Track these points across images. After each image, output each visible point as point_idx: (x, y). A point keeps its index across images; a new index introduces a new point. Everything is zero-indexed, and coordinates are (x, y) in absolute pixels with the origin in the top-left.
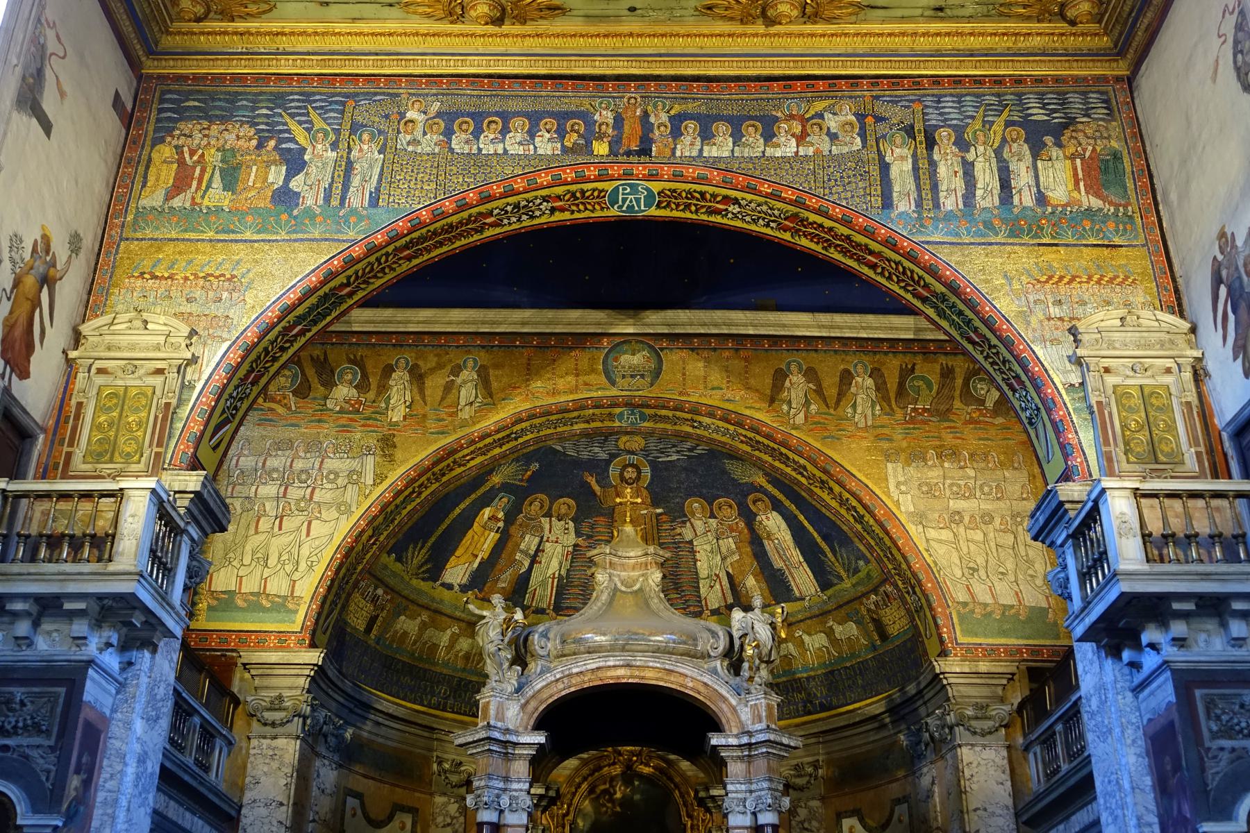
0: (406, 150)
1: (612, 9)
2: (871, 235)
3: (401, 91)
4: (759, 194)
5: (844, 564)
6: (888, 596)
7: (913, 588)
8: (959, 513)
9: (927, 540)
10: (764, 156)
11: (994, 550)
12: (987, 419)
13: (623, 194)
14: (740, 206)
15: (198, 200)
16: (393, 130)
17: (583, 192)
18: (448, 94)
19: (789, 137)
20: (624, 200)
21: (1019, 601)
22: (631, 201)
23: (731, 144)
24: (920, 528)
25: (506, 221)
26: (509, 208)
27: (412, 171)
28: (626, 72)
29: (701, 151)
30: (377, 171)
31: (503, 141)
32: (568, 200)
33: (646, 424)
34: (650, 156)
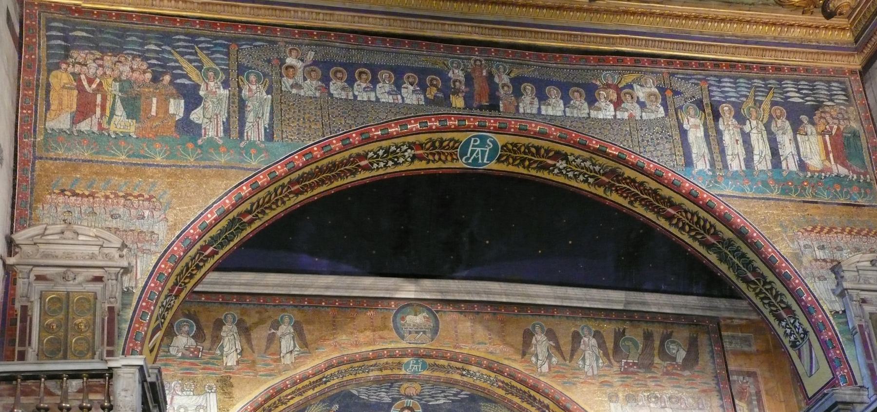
13: (474, 146)
14: (567, 161)
15: (105, 126)
17: (442, 141)
20: (473, 152)
22: (477, 154)
33: (425, 373)
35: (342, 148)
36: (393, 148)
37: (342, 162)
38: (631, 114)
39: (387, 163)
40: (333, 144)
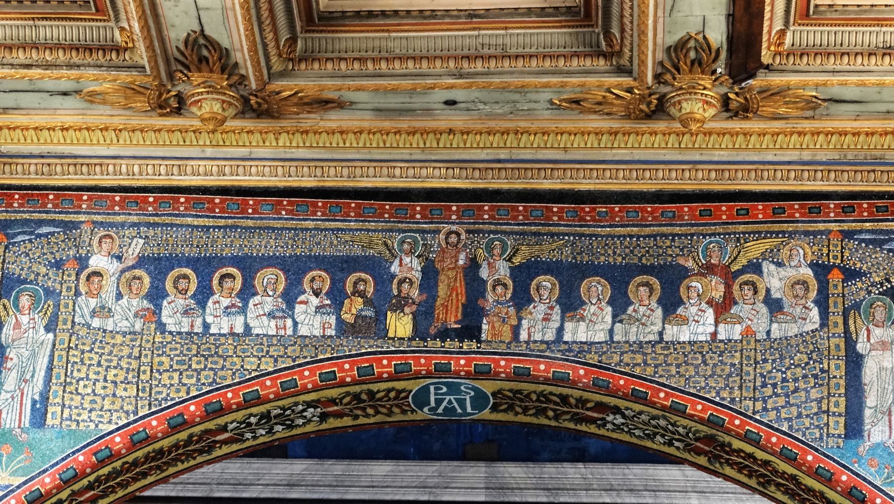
0: (89, 326)
1: (418, 102)
2: (829, 480)
3: (82, 218)
4: (653, 405)
10: (662, 339)
13: (436, 394)
14: (624, 416)
16: (69, 289)
17: (371, 394)
18: (155, 225)
19: (704, 306)
20: (439, 402)
22: (450, 402)
23: (609, 319)
25: (248, 435)
26: (253, 420)
27: (99, 364)
28: (445, 185)
29: (560, 330)
30: (42, 363)
31: (243, 310)
32: (349, 403)
34: (479, 341)
35: (168, 432)
36: (275, 412)
37: (176, 446)
38: (748, 327)
39: (272, 428)
40: (152, 428)
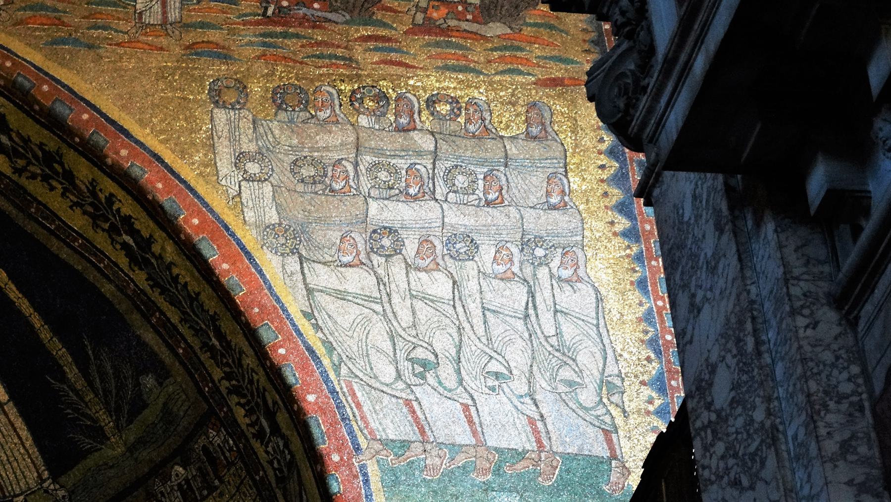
5: (106, 392)
6: (213, 461)
7: (271, 416)
8: (391, 231)
9: (310, 291)
11: (477, 321)
12: (464, 25)
21: (539, 441)
24: (293, 264)
